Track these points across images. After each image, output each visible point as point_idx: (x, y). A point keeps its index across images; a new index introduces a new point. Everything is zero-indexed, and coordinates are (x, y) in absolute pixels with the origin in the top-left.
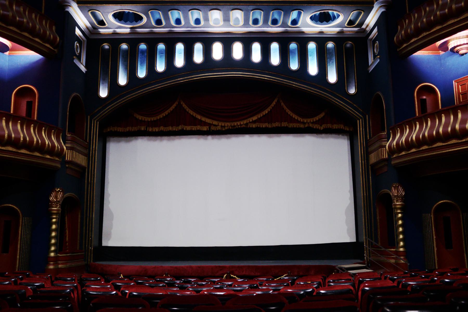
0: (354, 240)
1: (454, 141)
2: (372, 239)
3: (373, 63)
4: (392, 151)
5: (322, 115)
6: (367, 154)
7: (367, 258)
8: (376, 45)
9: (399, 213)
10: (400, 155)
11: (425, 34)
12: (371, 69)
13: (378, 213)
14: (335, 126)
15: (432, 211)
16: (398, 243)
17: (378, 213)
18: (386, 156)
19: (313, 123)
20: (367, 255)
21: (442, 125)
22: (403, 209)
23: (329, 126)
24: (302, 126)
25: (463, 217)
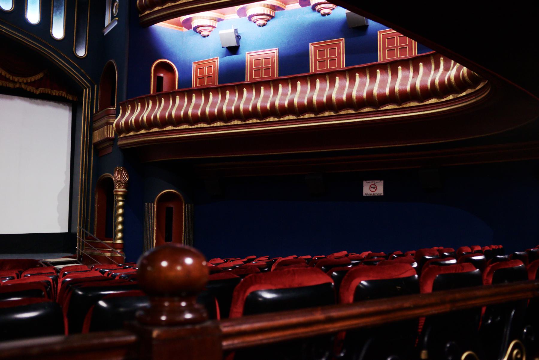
0: (66, 231)
1: (185, 127)
2: (87, 229)
3: (109, 25)
4: (119, 130)
5: (40, 76)
6: (91, 130)
7: (79, 251)
8: (116, 4)
9: (121, 201)
10: (128, 135)
11: (170, 4)
12: (107, 31)
13: (97, 200)
14: (55, 93)
15: (156, 200)
16: (116, 235)
17: (97, 200)
18: (112, 135)
19: (27, 84)
20: (79, 248)
21: (177, 107)
22: (126, 197)
23: (48, 91)
24: (11, 85)
25: (185, 208)
